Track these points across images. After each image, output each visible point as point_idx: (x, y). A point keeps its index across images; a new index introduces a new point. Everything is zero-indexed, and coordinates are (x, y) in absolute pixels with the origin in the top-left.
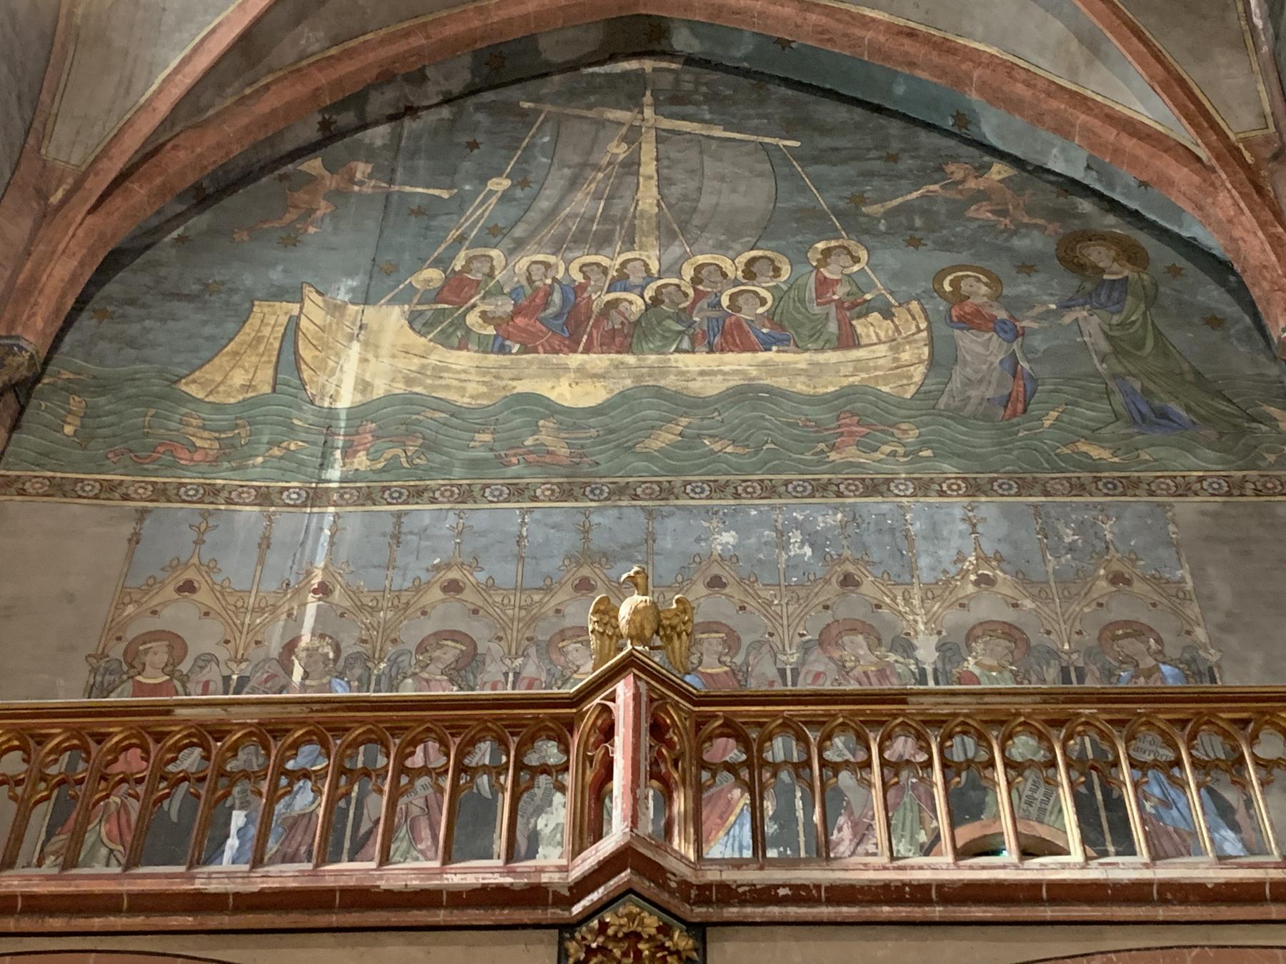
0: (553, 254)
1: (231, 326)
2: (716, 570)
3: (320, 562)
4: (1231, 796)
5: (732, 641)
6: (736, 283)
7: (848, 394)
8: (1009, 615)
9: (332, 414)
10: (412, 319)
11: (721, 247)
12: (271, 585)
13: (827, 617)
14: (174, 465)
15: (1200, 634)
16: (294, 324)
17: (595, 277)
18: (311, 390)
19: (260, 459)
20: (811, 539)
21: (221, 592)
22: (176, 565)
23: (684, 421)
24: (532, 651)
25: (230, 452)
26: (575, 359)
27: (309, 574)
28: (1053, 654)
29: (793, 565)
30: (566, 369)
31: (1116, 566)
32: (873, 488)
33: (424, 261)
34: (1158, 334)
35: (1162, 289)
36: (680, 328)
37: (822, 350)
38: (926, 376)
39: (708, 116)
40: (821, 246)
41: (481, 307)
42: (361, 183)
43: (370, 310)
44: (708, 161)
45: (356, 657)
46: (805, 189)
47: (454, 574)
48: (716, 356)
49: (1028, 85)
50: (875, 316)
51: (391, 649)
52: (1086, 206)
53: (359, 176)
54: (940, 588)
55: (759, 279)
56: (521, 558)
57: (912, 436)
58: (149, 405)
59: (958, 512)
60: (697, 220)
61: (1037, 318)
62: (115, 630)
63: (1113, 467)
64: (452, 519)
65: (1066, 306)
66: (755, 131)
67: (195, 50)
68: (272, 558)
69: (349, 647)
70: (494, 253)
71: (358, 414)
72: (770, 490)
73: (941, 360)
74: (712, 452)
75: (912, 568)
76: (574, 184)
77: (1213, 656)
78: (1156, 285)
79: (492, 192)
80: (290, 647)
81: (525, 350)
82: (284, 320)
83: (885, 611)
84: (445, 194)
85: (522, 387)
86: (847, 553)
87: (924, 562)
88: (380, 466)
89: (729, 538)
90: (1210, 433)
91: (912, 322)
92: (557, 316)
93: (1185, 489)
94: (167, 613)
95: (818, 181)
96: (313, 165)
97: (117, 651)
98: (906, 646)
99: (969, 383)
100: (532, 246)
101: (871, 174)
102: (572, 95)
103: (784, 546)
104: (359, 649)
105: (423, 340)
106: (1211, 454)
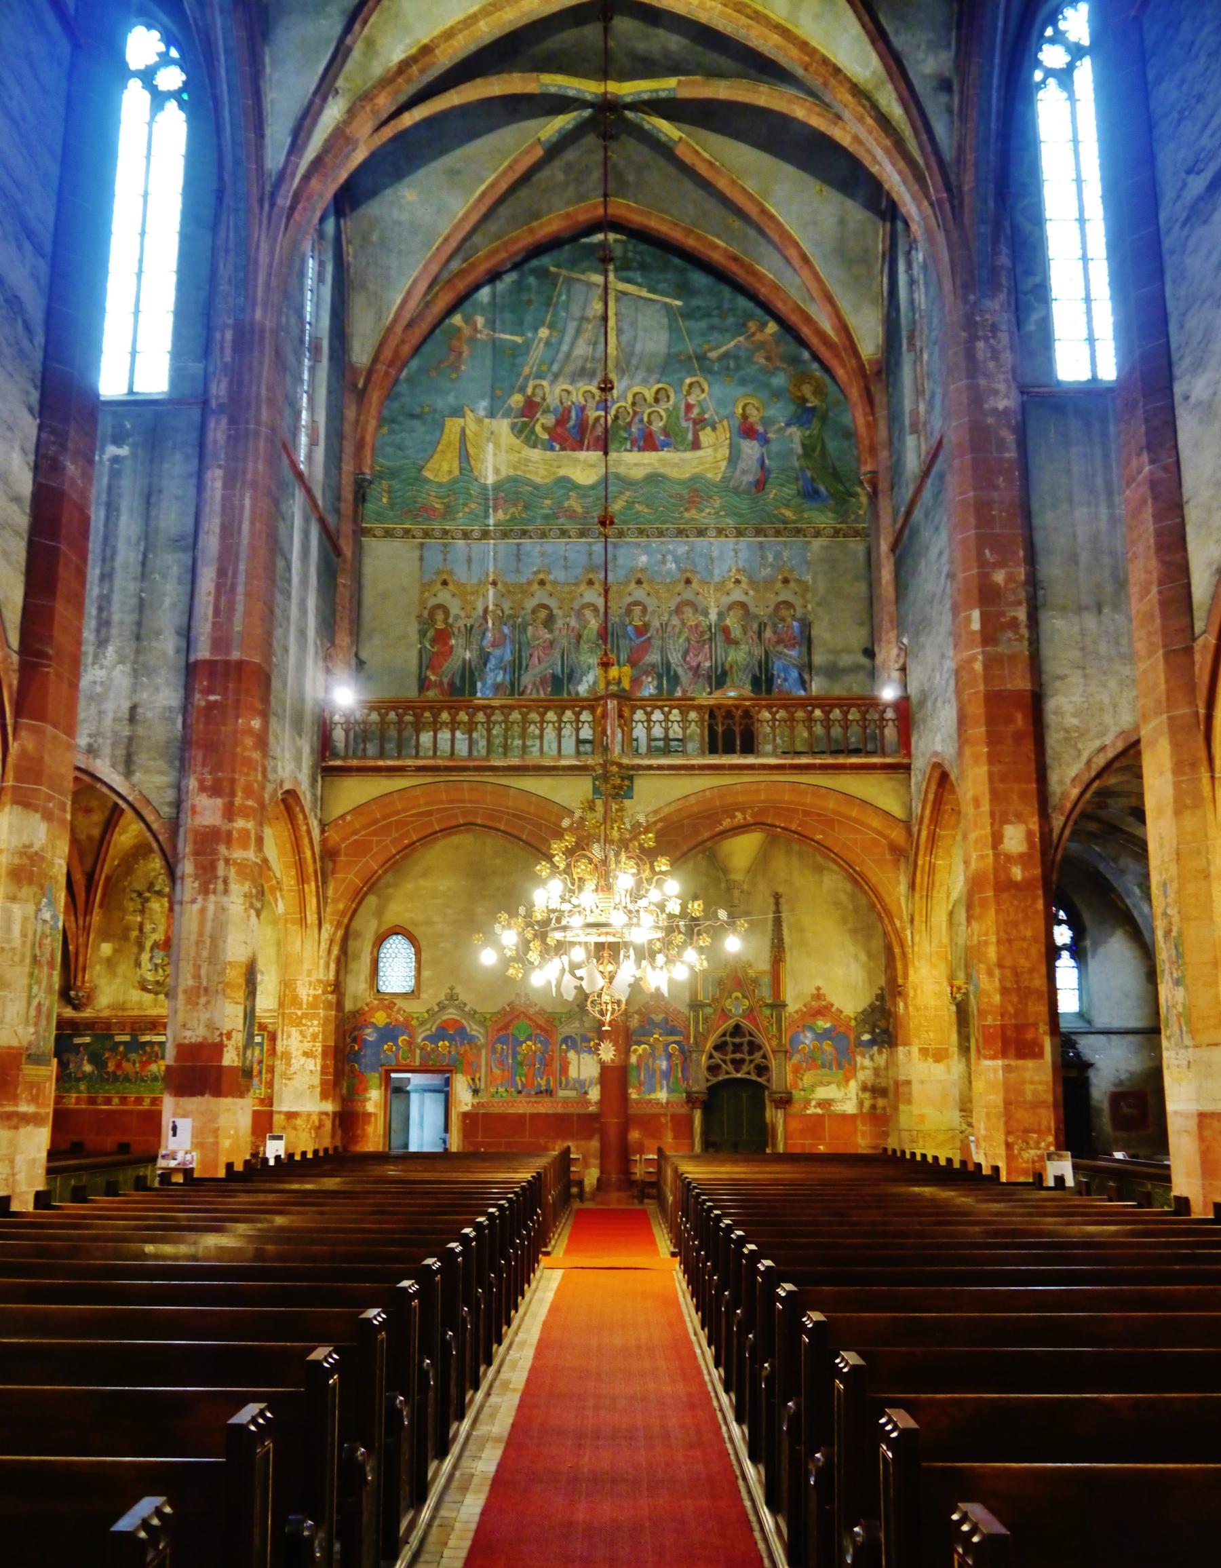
0: (572, 382)
1: (437, 434)
2: (639, 575)
3: (491, 570)
4: (806, 677)
5: (644, 611)
6: (651, 406)
7: (695, 479)
8: (743, 598)
9: (484, 487)
10: (513, 426)
11: (645, 382)
12: (475, 581)
13: (678, 599)
14: (430, 519)
15: (810, 607)
16: (463, 430)
17: (590, 400)
18: (476, 473)
19: (460, 515)
20: (676, 561)
21: (458, 584)
22: (439, 573)
23: (628, 493)
24: (573, 614)
25: (449, 512)
26: (583, 455)
27: (487, 575)
28: (756, 616)
29: (669, 572)
30: (577, 460)
31: (786, 574)
32: (701, 533)
33: (513, 387)
34: (823, 441)
35: (831, 414)
36: (626, 435)
37: (685, 450)
38: (727, 468)
39: (640, 280)
40: (688, 381)
41: (543, 420)
42: (481, 332)
43: (494, 422)
44: (640, 317)
45: (510, 616)
46: (683, 340)
47: (541, 576)
48: (641, 453)
49: (785, 304)
50: (708, 429)
51: (523, 613)
52: (806, 355)
53: (479, 326)
54: (720, 586)
55: (662, 403)
56: (566, 568)
57: (717, 505)
58: (410, 484)
59: (731, 546)
60: (634, 361)
61: (777, 431)
62: (423, 603)
63: (794, 522)
64: (538, 548)
65: (788, 425)
66: (662, 293)
67: (409, 294)
68: (474, 567)
69: (508, 612)
70: (545, 383)
71: (497, 487)
72: (661, 534)
73: (733, 459)
74: (638, 512)
75: (711, 573)
76: (578, 331)
77: (811, 618)
78: (827, 411)
79: (541, 339)
80: (486, 611)
81: (563, 449)
82: (459, 429)
83: (700, 597)
84: (518, 339)
85: (562, 472)
86: (688, 567)
87: (716, 572)
88: (508, 517)
89: (644, 559)
90: (832, 502)
91: (723, 435)
92: (574, 427)
93: (817, 534)
94: (439, 595)
95: (689, 332)
96: (457, 319)
97: (426, 614)
98: (706, 613)
99: (744, 472)
100: (561, 379)
101: (712, 328)
102: (573, 263)
103: (664, 562)
104: (510, 612)
105: (518, 442)
106: (830, 515)
